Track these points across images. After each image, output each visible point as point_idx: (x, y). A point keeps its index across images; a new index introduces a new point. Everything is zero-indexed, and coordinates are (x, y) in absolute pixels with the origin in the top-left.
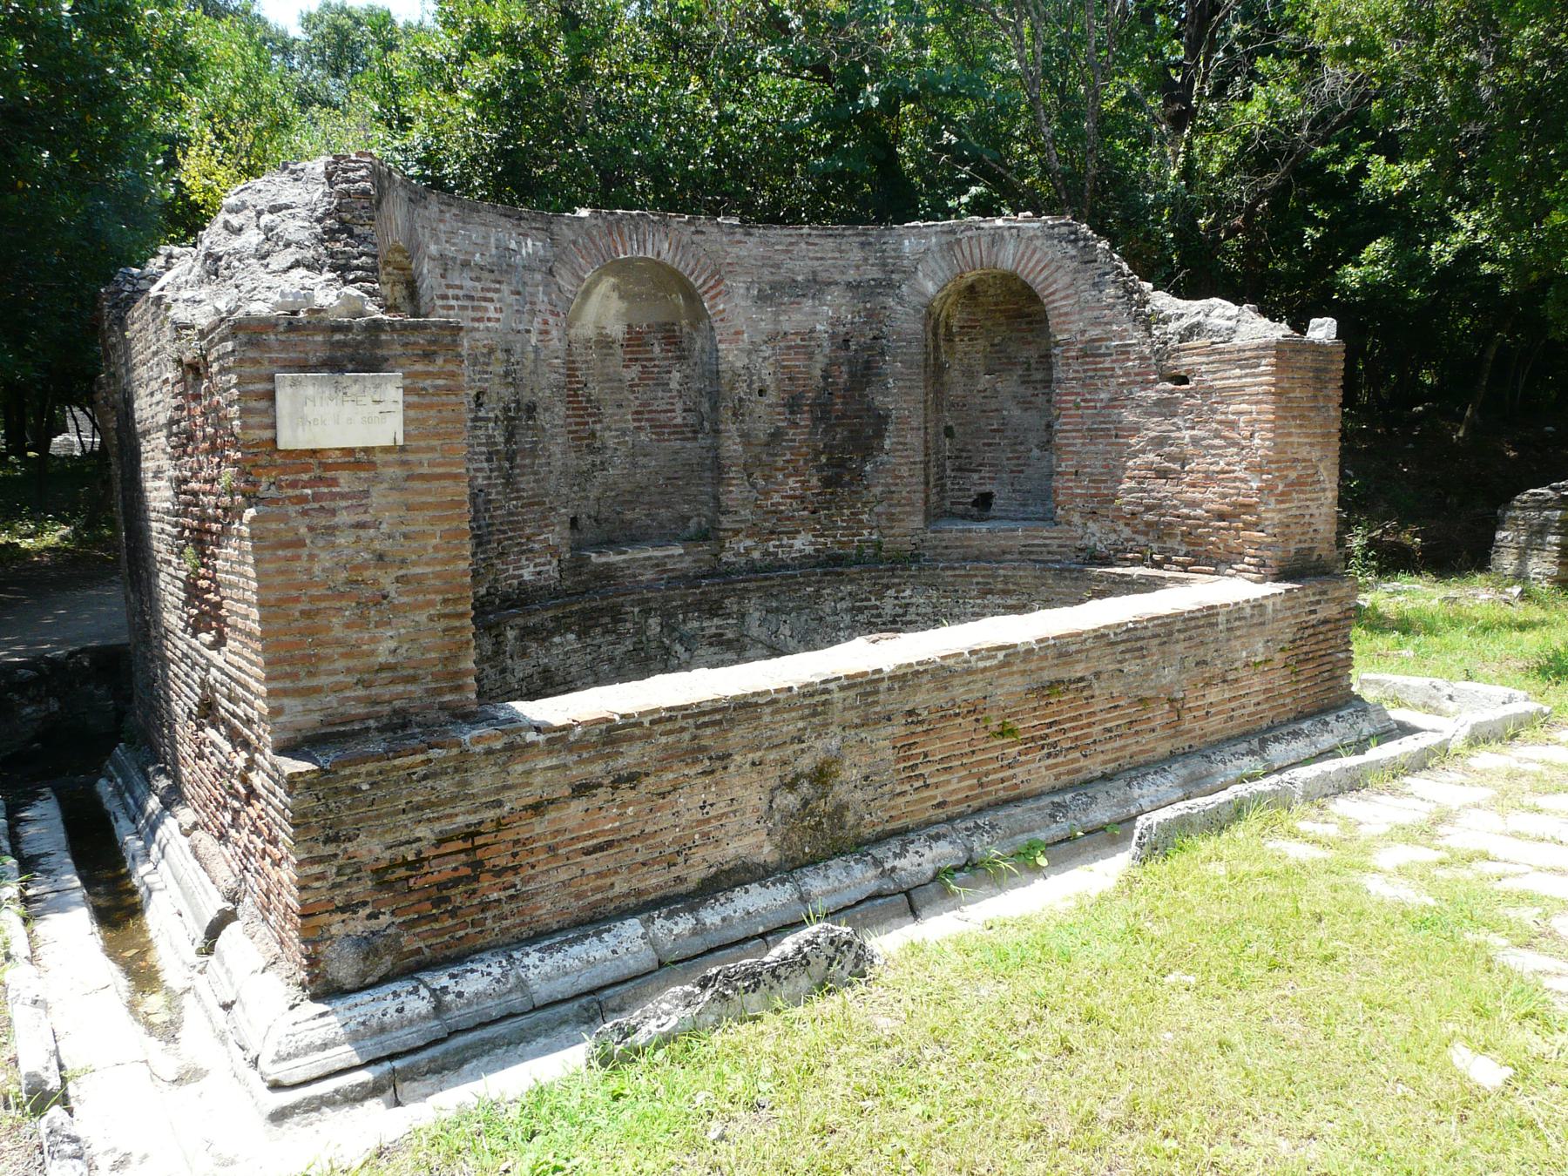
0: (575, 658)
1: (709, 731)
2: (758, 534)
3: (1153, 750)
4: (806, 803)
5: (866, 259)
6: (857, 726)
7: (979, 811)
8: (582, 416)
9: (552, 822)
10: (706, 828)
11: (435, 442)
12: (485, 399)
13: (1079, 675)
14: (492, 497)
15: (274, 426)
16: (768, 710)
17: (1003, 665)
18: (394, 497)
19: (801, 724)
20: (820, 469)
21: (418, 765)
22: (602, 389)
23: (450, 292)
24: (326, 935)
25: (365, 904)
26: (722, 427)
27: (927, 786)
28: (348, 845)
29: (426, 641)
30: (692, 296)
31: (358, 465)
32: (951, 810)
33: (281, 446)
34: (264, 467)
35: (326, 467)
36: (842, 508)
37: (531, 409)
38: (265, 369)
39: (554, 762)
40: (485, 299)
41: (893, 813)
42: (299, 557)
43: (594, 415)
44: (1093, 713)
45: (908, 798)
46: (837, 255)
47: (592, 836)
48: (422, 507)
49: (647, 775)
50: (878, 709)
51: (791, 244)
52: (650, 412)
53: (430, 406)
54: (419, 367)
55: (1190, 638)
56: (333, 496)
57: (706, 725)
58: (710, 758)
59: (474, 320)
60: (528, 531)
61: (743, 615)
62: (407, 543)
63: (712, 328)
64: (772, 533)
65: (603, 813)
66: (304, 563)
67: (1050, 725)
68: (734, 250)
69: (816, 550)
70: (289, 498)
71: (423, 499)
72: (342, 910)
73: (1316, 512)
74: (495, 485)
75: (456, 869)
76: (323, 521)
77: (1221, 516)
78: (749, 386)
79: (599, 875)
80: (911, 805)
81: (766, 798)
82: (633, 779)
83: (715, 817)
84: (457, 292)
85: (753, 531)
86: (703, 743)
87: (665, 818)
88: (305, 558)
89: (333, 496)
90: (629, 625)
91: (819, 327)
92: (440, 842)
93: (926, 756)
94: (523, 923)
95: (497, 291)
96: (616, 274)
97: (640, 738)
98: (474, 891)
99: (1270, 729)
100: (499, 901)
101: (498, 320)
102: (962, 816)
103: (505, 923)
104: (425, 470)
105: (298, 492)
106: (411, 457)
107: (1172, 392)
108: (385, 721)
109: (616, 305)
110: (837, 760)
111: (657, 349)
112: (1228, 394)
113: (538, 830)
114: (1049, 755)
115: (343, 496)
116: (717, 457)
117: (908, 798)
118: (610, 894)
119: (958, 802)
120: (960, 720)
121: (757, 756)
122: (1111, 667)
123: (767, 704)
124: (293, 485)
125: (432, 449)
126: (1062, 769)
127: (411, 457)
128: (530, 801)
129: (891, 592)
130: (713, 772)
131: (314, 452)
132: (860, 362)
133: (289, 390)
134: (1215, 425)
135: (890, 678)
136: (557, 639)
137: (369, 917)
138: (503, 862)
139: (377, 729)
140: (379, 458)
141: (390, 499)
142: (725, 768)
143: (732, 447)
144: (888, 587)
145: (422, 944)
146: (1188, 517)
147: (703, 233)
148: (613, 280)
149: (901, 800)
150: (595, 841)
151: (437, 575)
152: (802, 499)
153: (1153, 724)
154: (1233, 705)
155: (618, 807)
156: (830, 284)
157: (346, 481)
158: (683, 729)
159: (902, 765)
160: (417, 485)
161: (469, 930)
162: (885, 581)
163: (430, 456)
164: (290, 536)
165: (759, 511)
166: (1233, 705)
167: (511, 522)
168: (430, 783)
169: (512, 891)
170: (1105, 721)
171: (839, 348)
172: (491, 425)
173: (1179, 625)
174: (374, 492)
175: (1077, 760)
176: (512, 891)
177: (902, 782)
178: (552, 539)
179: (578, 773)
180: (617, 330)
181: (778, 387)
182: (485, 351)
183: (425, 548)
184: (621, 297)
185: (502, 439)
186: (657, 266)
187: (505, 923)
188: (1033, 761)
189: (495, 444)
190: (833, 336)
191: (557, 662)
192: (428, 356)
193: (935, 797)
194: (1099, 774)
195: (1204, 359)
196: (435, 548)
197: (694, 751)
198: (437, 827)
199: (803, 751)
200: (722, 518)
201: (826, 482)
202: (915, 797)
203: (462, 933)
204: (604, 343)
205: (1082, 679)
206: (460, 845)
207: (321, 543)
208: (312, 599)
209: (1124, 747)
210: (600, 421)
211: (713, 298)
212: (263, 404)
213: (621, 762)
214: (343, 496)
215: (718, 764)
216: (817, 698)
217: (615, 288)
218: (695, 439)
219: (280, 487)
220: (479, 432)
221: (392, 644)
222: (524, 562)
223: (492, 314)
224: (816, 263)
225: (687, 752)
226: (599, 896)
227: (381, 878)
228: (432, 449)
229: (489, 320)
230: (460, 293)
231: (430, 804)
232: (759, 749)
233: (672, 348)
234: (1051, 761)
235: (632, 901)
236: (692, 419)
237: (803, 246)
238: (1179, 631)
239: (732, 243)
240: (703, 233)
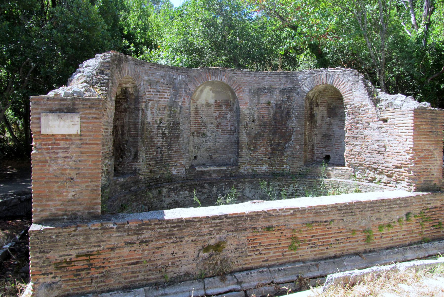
0: (187, 199)
1: (176, 229)
2: (251, 164)
3: (358, 248)
4: (211, 256)
5: (287, 82)
6: (233, 231)
7: (282, 264)
8: (199, 126)
9: (117, 253)
10: (174, 261)
11: (91, 134)
12: (163, 121)
13: (325, 220)
14: (163, 149)
15: (40, 127)
16: (199, 224)
17: (292, 215)
18: (77, 149)
19: (211, 229)
20: (271, 145)
21: (72, 232)
22: (207, 119)
23: (152, 90)
24: (38, 282)
25: (51, 273)
26: (240, 131)
27: (261, 254)
28: (47, 254)
29: (85, 193)
30: (233, 93)
31: (67, 140)
32: (270, 263)
33: (42, 133)
34: (37, 139)
35: (56, 140)
36: (278, 157)
37: (178, 124)
38: (39, 111)
39: (119, 234)
40: (164, 92)
41: (247, 262)
42: (45, 166)
43: (204, 126)
44: (331, 234)
45: (253, 257)
46: (278, 80)
47: (131, 259)
48: (86, 152)
49: (152, 241)
50: (241, 226)
51: (264, 77)
52: (221, 126)
53: (90, 123)
54: (88, 111)
55: (373, 210)
56: (58, 148)
57: (175, 227)
58: (176, 238)
59: (159, 98)
60: (175, 160)
61: (244, 189)
62: (80, 163)
63: (238, 102)
64: (255, 164)
65: (136, 252)
66: (47, 168)
67: (313, 237)
68: (246, 79)
69: (269, 171)
70: (44, 148)
71: (86, 150)
72: (44, 274)
73: (432, 168)
74: (164, 146)
75: (83, 265)
76: (53, 155)
77: (397, 167)
78: (250, 119)
79: (133, 272)
80: (252, 260)
81: (197, 252)
82: (147, 242)
83: (177, 257)
84: (154, 90)
85: (250, 163)
86: (174, 232)
87: (158, 256)
88: (47, 166)
89: (58, 148)
90: (206, 190)
91: (272, 102)
92: (78, 256)
93: (260, 243)
94: (105, 285)
95: (169, 90)
96: (211, 85)
97: (150, 229)
98: (89, 273)
99: (409, 245)
100: (97, 277)
101: (168, 98)
102: (274, 265)
103: (99, 285)
104: (88, 142)
105: (47, 147)
106: (83, 138)
107: (382, 125)
108: (69, 217)
109: (212, 95)
110: (225, 242)
111: (224, 107)
112: (399, 126)
113: (112, 255)
114: (312, 247)
115: (61, 148)
116: (238, 140)
117: (253, 257)
118: (137, 279)
119: (273, 260)
120: (274, 232)
121: (194, 238)
122: (338, 218)
123: (198, 221)
124: (45, 145)
125: (91, 136)
126: (317, 252)
127: (83, 138)
128: (110, 246)
129: (292, 185)
130: (177, 242)
131: (53, 135)
132: (282, 114)
133: (44, 117)
134: (395, 137)
135: (246, 216)
136: (181, 193)
137: (53, 277)
138: (100, 264)
139: (67, 219)
140: (73, 138)
141: (75, 150)
142: (182, 241)
143: (244, 138)
144: (290, 183)
145: (70, 288)
146: (387, 167)
147: (236, 73)
148: (210, 87)
149: (250, 258)
150: (133, 261)
151: (89, 173)
152: (265, 154)
153: (357, 239)
154: (393, 235)
155: (142, 251)
156: (275, 89)
157: (62, 144)
158: (166, 228)
159: (250, 246)
160: (85, 146)
161: (86, 285)
162: (290, 182)
163: (90, 137)
164: (43, 159)
165: (251, 157)
166: (393, 235)
167: (169, 157)
168: (75, 237)
169: (102, 274)
170: (336, 237)
171: (278, 108)
172: (164, 128)
173: (367, 205)
174: (71, 147)
175: (324, 250)
176: (102, 274)
177: (250, 252)
178: (183, 163)
179: (127, 239)
180: (212, 102)
181: (259, 119)
182: (164, 107)
183: (86, 165)
184: (213, 92)
185: (168, 133)
186: (222, 83)
187: (99, 285)
188: (305, 249)
189: (165, 134)
190: (276, 105)
191: (181, 200)
192: (91, 108)
193: (264, 258)
194: (333, 255)
195: (391, 114)
196: (90, 165)
197: (170, 235)
198: (77, 251)
199: (211, 238)
200: (239, 159)
201: (273, 150)
202: (256, 257)
203: (84, 286)
204: (208, 105)
205: (326, 221)
206: (85, 258)
207: (53, 162)
208: (49, 178)
209: (345, 246)
210: (206, 128)
211: (239, 92)
212: (38, 121)
213: (143, 236)
214: (61, 148)
215: (178, 240)
216: (217, 221)
217: (211, 89)
218: (233, 134)
219: (42, 145)
220: (159, 130)
221: (74, 193)
222: (173, 169)
223: (166, 97)
224: (272, 83)
225: (167, 235)
226: (133, 279)
227: (58, 266)
228: (91, 136)
229: (165, 98)
230: (155, 90)
231: (75, 244)
232: (195, 236)
233: (228, 107)
234: (312, 249)
235: (145, 282)
236: (233, 128)
237: (268, 77)
238: (368, 207)
239: (245, 77)
240: (236, 73)
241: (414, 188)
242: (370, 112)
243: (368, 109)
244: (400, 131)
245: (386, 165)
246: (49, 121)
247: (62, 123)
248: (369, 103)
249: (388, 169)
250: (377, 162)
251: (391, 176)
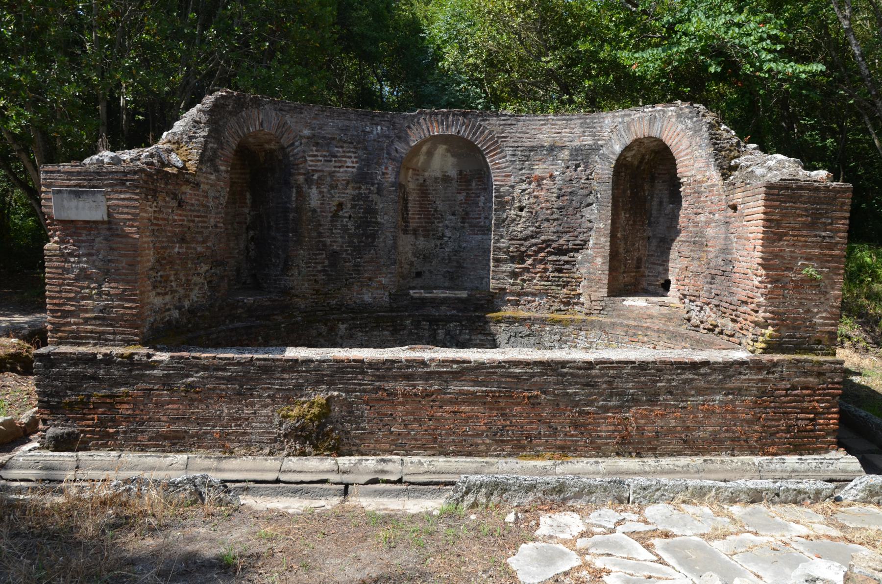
35: (77, 228)
43: (439, 218)
59: (335, 167)
95: (355, 153)
96: (445, 144)
101: (354, 167)
109: (451, 160)
129: (583, 333)
131: (72, 221)
148: (444, 147)
180: (453, 173)
184: (452, 156)
204: (446, 179)
217: (448, 150)
229: (348, 167)
241: (763, 345)
243: (713, 186)
246: (63, 201)
247: (81, 204)
248: (714, 173)
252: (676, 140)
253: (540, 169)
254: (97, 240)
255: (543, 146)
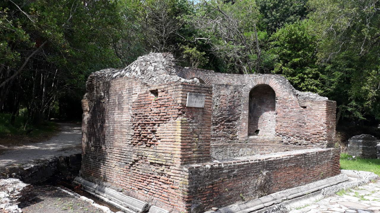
107: (302, 110)
129: (241, 149)
241: (326, 146)
242: (294, 102)
244: (316, 113)
245: (306, 134)
249: (307, 136)
250: (299, 132)
251: (310, 141)
252: (275, 86)
253: (222, 92)
254: (199, 116)
255: (224, 84)
